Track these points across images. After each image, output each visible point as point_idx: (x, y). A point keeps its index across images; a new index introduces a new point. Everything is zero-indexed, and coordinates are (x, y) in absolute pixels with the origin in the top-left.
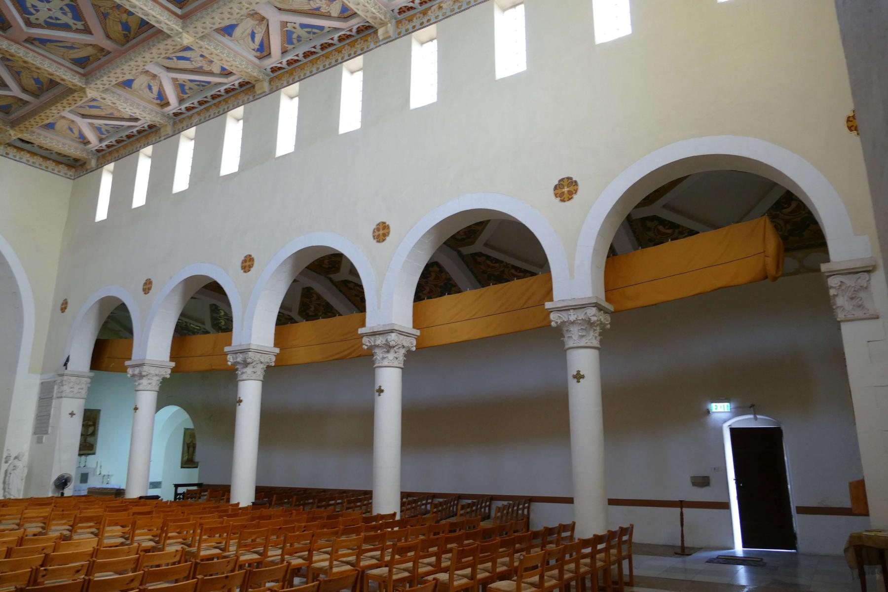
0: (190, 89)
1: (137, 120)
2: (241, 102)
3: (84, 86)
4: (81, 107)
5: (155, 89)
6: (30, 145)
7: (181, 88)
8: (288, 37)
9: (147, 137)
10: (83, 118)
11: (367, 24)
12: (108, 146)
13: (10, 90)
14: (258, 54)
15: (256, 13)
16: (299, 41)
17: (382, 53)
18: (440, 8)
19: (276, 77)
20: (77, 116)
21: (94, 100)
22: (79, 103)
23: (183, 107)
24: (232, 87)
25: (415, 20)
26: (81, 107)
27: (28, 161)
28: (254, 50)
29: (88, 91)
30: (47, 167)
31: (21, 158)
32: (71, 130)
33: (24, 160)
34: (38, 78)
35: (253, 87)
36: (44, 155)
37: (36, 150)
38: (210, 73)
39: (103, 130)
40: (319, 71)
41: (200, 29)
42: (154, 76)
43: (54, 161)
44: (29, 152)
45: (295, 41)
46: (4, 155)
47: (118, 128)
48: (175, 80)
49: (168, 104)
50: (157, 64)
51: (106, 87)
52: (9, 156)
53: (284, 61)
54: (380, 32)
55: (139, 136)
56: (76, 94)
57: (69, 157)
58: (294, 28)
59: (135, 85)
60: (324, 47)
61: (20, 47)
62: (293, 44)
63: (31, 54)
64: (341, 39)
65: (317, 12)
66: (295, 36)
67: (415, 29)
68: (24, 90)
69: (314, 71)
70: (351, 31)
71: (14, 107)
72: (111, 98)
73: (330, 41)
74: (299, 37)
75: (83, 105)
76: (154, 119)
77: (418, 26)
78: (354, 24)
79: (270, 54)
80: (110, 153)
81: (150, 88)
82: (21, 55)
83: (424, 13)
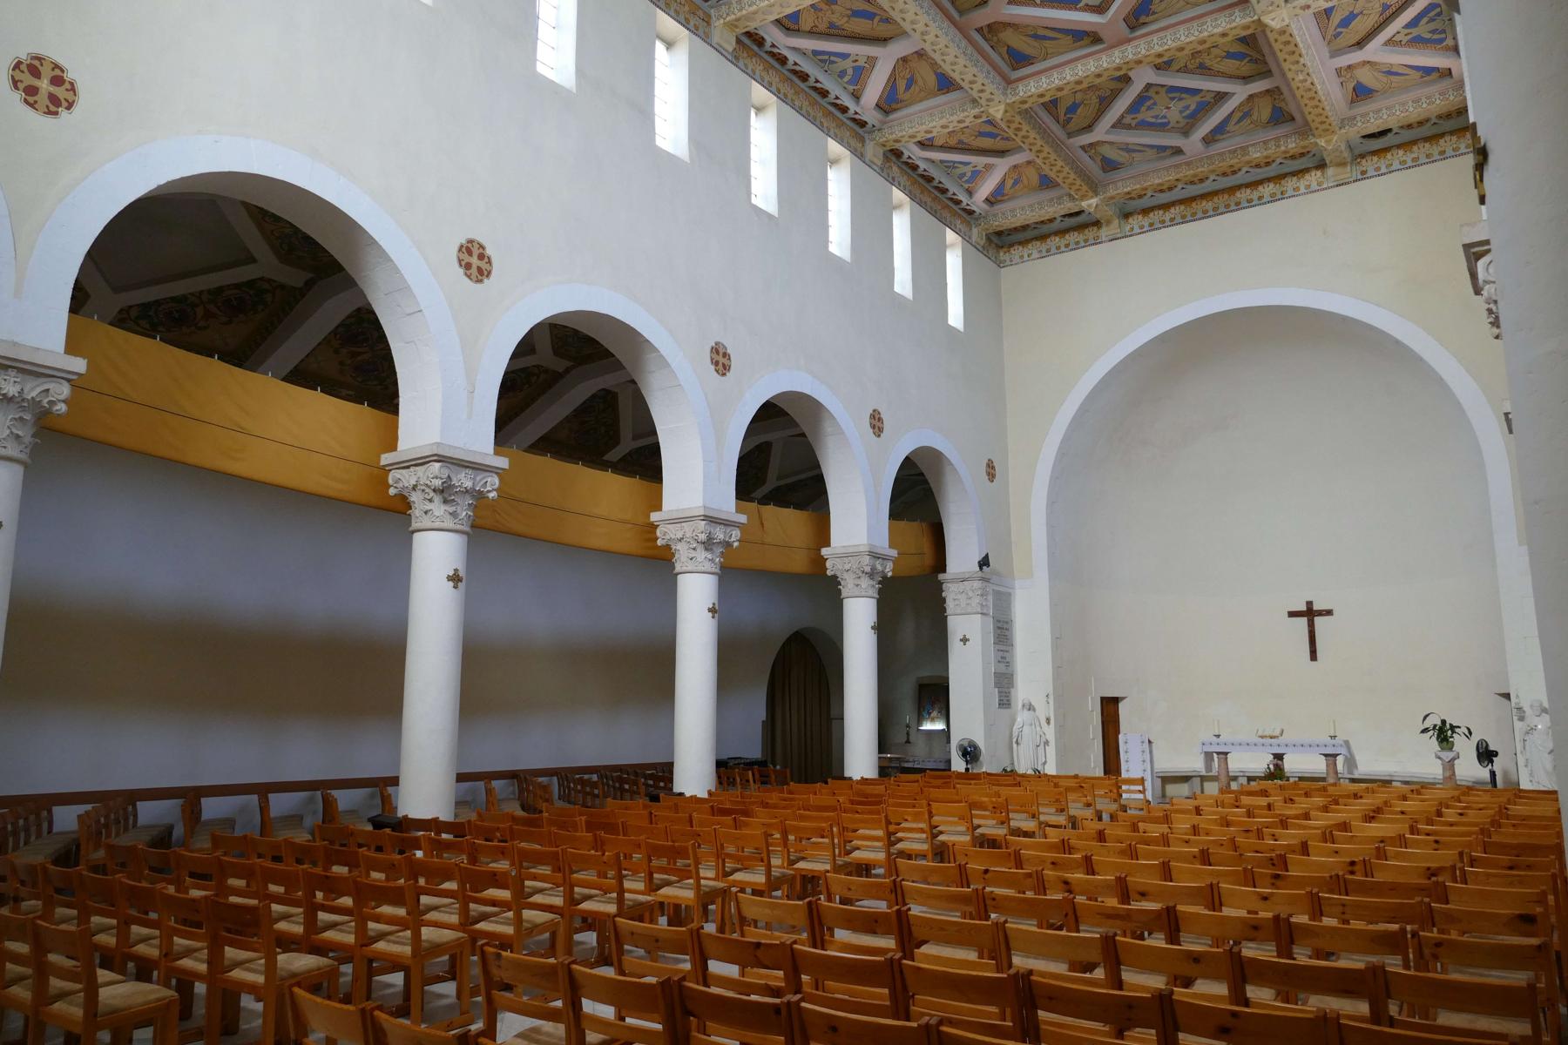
3: (1256, 18)
6: (1389, 135)
10: (1361, 48)
13: (1234, 94)
20: (1350, 52)
29: (1266, 20)
30: (1442, 153)
32: (1390, 73)
34: (1228, 52)
36: (1429, 134)
37: (1407, 135)
39: (1428, 36)
43: (1452, 133)
44: (1399, 146)
46: (1360, 177)
61: (1135, 43)
63: (1155, 38)
68: (1246, 79)
71: (1282, 105)
82: (1143, 52)
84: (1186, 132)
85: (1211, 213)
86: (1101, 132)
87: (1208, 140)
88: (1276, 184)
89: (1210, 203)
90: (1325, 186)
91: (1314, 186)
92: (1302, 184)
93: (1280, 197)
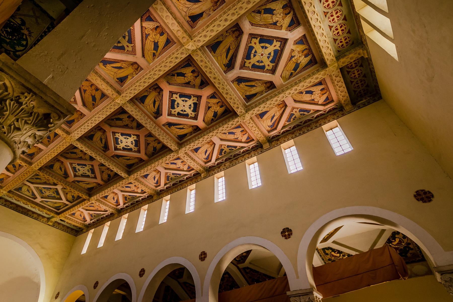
0: (129, 198)
1: (107, 211)
2: (147, 203)
4: (87, 206)
5: (116, 199)
7: (125, 198)
8: (168, 178)
9: (109, 218)
11: (197, 173)
12: (93, 222)
14: (156, 185)
15: (157, 170)
16: (171, 179)
17: (204, 182)
18: (225, 165)
19: (162, 193)
21: (92, 203)
22: (86, 205)
23: (125, 206)
24: (145, 198)
25: (215, 170)
26: (87, 206)
27: (61, 228)
28: (154, 183)
30: (68, 231)
31: (59, 227)
33: (60, 228)
35: (153, 197)
37: (65, 224)
38: (137, 193)
39: (93, 215)
40: (178, 190)
41: (135, 176)
42: (116, 194)
45: (170, 180)
47: (98, 215)
48: (123, 195)
49: (119, 205)
50: (118, 189)
51: (98, 198)
52: (54, 227)
53: (165, 187)
54: (202, 175)
55: (106, 218)
56: (86, 201)
57: (77, 227)
58: (170, 175)
59: (108, 198)
60: (180, 181)
62: (169, 180)
64: (187, 179)
65: (179, 169)
66: (170, 178)
67: (215, 173)
68: (67, 200)
69: (177, 190)
70: (191, 175)
72: (98, 203)
73: (183, 179)
74: (171, 178)
75: (87, 206)
76: (113, 211)
77: (217, 172)
78: (192, 172)
79: (160, 184)
80: (94, 225)
81: (114, 198)
83: (219, 167)
84: (42, 198)
85: (20, 212)
86: (32, 186)
87: (42, 202)
88: (38, 216)
89: (22, 210)
90: (46, 223)
91: (44, 222)
92: (42, 220)
93: (36, 219)
